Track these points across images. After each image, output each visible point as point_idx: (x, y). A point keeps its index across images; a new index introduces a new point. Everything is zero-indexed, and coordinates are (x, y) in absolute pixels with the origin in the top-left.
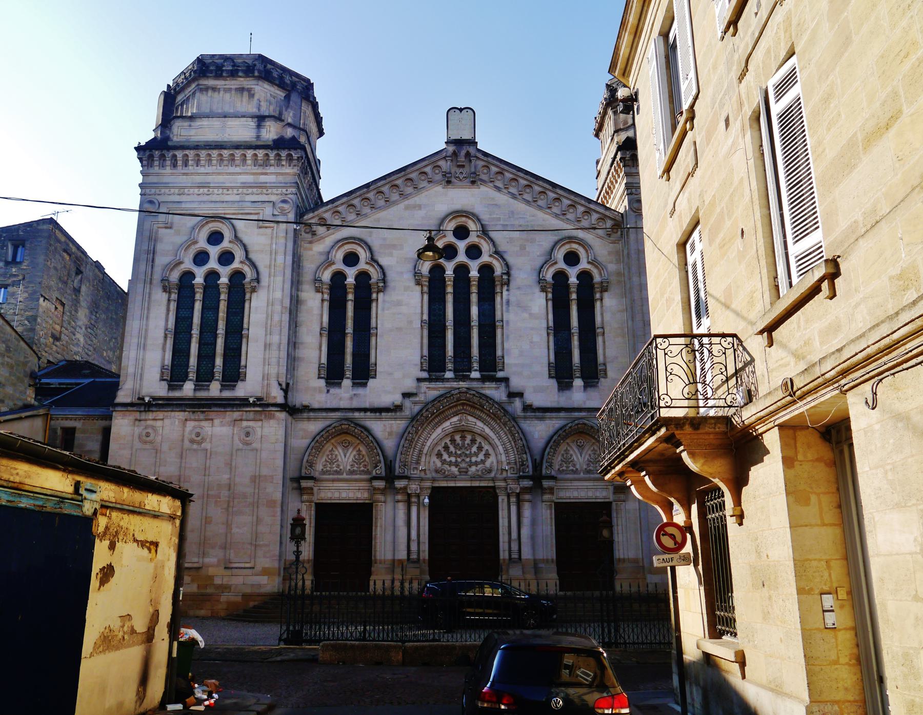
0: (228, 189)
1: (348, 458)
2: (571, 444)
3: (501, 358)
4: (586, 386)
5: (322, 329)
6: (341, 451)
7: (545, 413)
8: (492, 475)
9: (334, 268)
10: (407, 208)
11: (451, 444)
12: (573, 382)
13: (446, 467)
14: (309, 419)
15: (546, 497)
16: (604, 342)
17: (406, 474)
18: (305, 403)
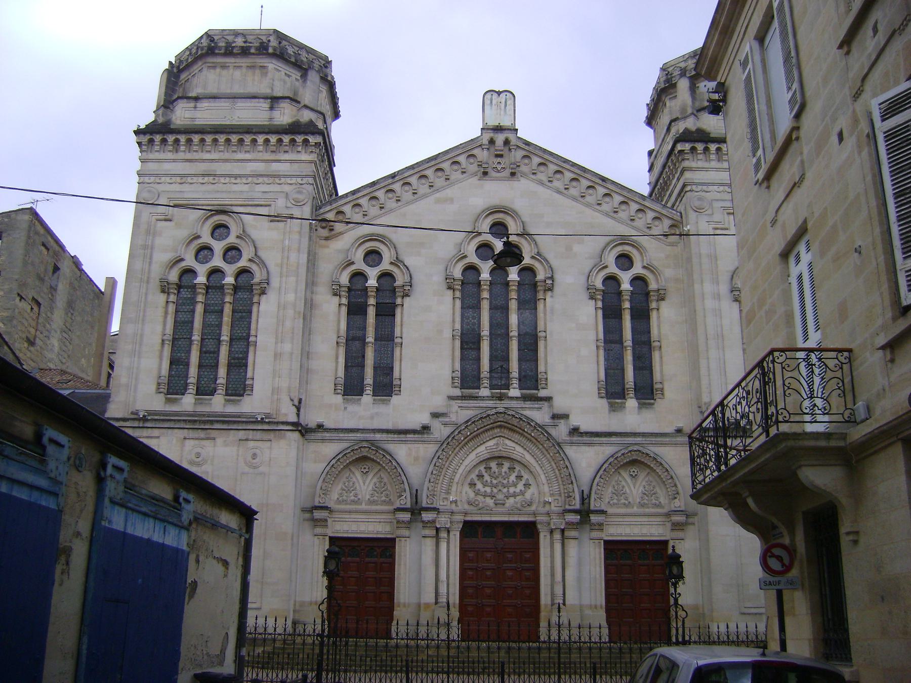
0: (236, 177)
1: (368, 486)
4: (642, 406)
8: (533, 508)
9: (353, 267)
10: (438, 201)
13: (480, 498)
14: (323, 440)
15: (595, 534)
16: (661, 357)
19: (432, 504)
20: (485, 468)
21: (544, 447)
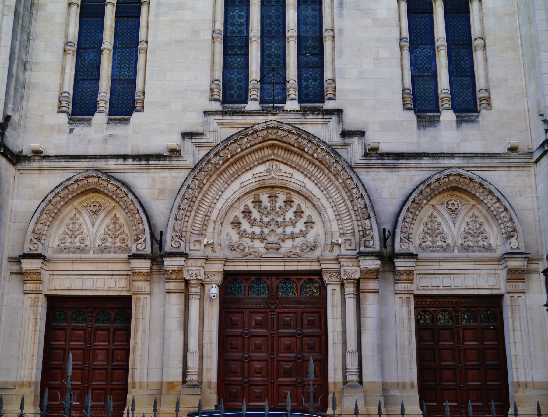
2: (438, 207)
3: (331, 82)
4: (460, 122)
5: (67, 44)
6: (87, 218)
7: (399, 160)
8: (318, 253)
11: (255, 207)
12: (439, 117)
13: (246, 241)
14: (41, 170)
15: (402, 286)
16: (486, 59)
17: (182, 249)
18: (36, 146)
19: (178, 248)
20: (253, 202)
21: (330, 171)
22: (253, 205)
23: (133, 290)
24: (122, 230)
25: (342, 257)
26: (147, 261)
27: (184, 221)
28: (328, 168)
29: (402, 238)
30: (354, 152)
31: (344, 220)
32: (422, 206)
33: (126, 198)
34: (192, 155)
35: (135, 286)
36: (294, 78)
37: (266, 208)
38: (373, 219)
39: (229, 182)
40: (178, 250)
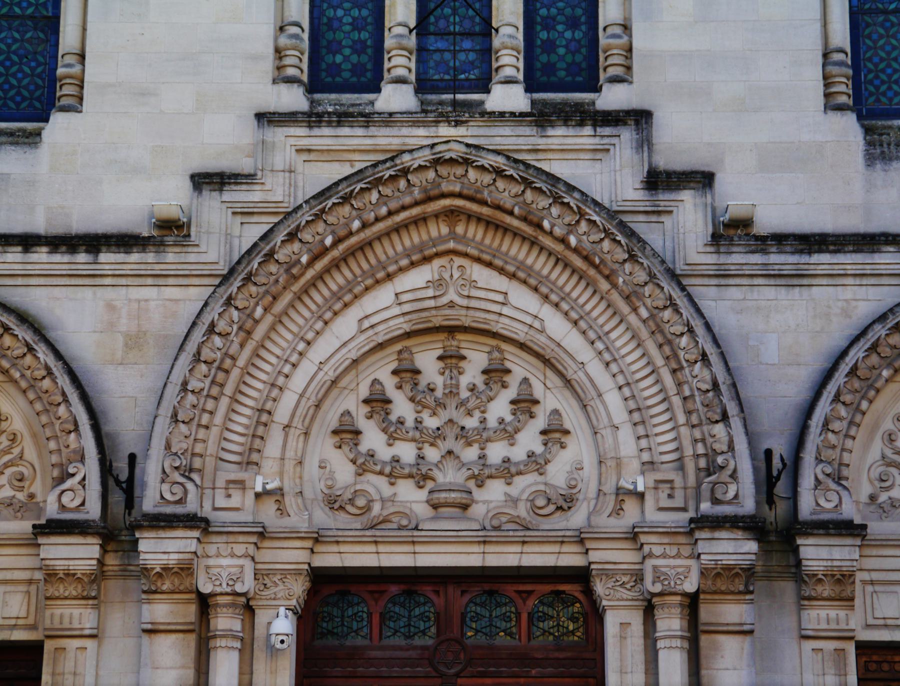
3: (618, 30)
7: (810, 253)
8: (577, 518)
11: (399, 387)
13: (375, 484)
17: (191, 506)
19: (180, 502)
20: (395, 372)
21: (615, 286)
22: (396, 380)
23: (48, 623)
24: (16, 451)
25: (646, 530)
26: (90, 540)
27: (199, 425)
28: (607, 277)
29: (821, 477)
30: (681, 231)
31: (655, 426)
32: (878, 385)
33: (29, 359)
34: (223, 239)
35: (52, 615)
36: (512, 20)
37: (432, 390)
38: (736, 423)
39: (328, 315)
40: (179, 510)
